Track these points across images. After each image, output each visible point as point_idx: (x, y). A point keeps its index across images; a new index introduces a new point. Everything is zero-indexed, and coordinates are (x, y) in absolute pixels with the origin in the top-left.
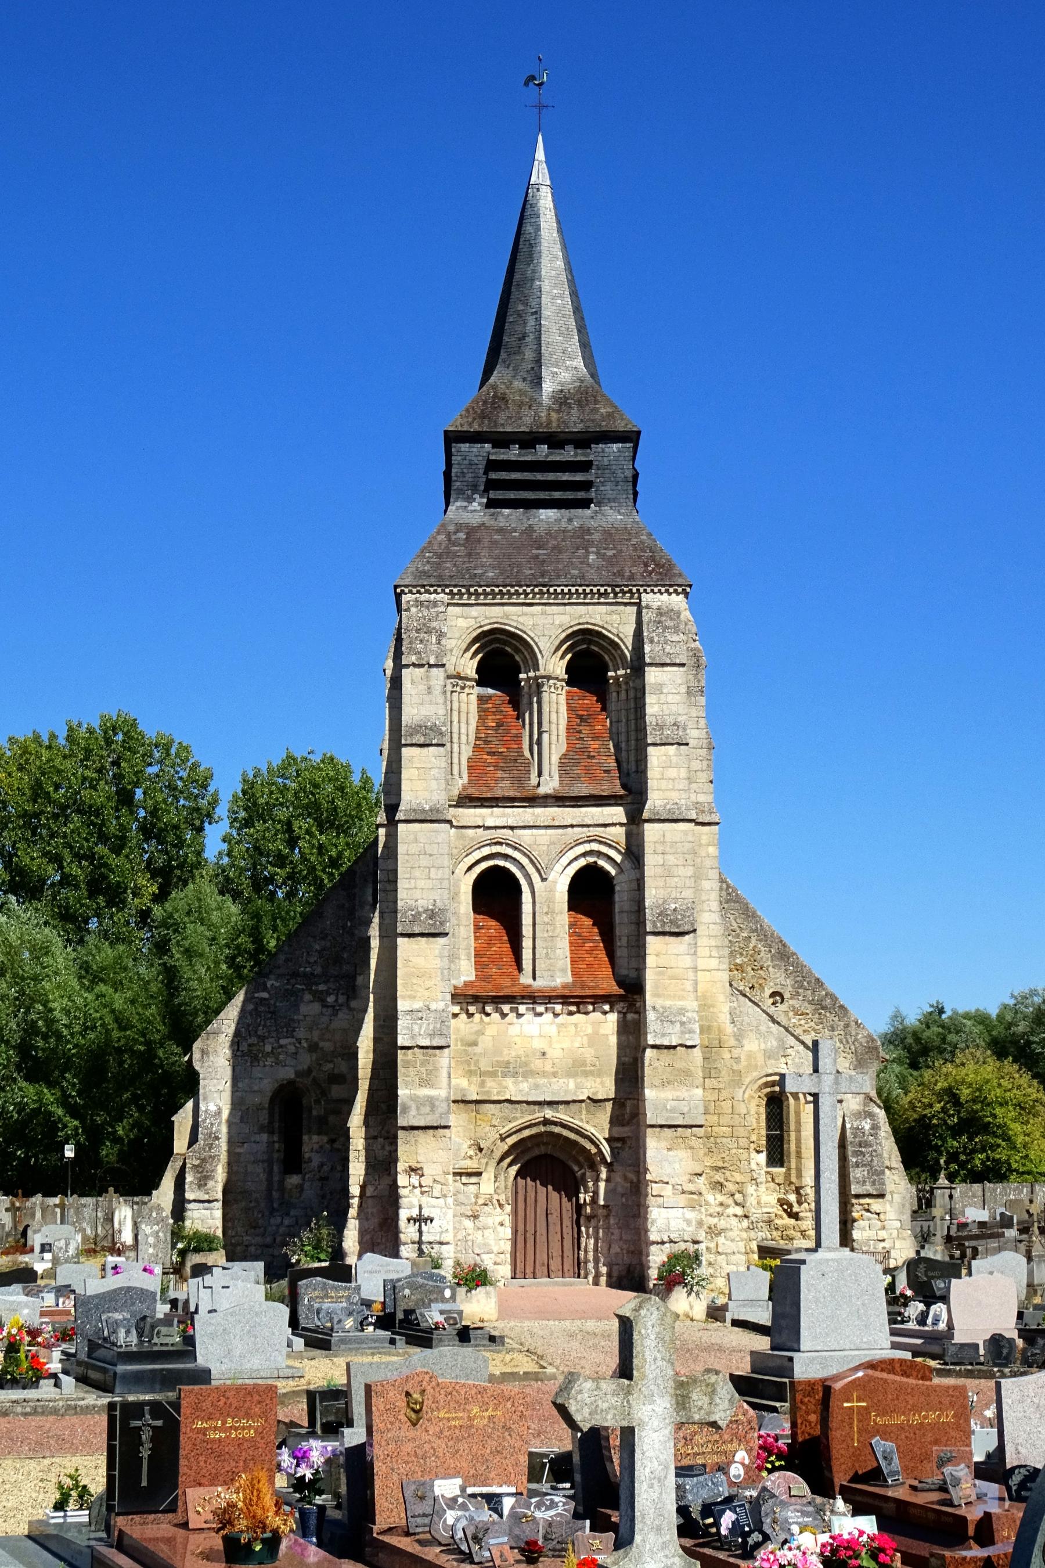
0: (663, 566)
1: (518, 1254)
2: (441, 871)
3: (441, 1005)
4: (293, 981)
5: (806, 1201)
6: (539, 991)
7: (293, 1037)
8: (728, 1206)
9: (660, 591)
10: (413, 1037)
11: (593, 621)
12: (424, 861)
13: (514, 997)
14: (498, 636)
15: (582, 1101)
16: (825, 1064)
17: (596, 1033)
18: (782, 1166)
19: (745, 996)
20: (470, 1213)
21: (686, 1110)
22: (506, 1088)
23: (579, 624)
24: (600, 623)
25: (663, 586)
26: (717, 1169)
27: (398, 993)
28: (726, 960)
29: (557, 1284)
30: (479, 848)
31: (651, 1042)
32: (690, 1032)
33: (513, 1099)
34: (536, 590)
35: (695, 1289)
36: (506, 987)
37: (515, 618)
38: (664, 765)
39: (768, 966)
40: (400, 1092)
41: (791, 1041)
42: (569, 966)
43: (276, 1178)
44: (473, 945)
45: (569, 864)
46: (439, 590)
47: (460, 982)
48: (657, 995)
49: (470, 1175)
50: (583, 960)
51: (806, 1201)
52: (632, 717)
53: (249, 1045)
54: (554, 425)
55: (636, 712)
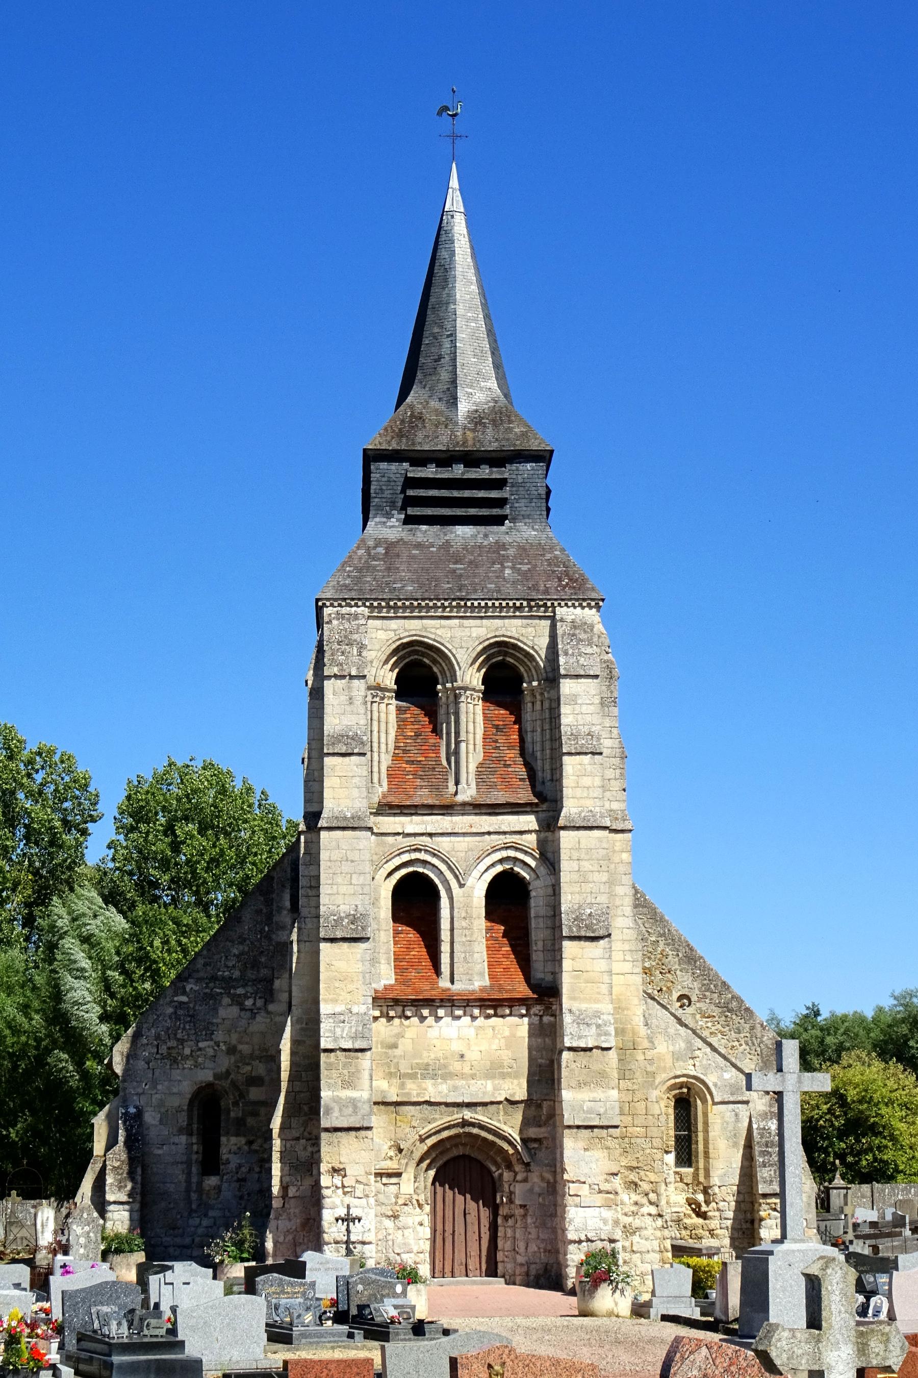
0: (577, 580)
1: (437, 1254)
2: (362, 878)
3: (362, 1009)
4: (211, 985)
5: (714, 1201)
6: (458, 994)
7: (212, 1040)
8: (642, 1205)
9: (573, 604)
10: (336, 1039)
11: (509, 634)
12: (346, 867)
13: (433, 1000)
14: (417, 648)
15: (499, 1103)
16: (789, 1064)
17: (513, 1035)
18: (690, 1166)
19: (653, 999)
20: (390, 1213)
21: (602, 1110)
22: (425, 1089)
23: (496, 636)
24: (516, 636)
25: (577, 600)
26: (632, 1169)
27: (321, 997)
28: (640, 964)
29: (475, 1283)
30: (399, 855)
31: (567, 1044)
32: (606, 1034)
33: (432, 1100)
34: (454, 603)
35: (620, 1286)
36: (426, 990)
37: (433, 630)
38: (578, 773)
39: (676, 970)
40: (323, 1094)
41: (699, 1043)
42: (487, 970)
43: (194, 1180)
44: (393, 949)
45: (486, 871)
46: (360, 603)
47: (380, 986)
48: (573, 999)
49: (390, 1175)
50: (500, 963)
51: (714, 1201)
52: (547, 727)
53: (169, 1048)
54: (470, 443)
55: (551, 722)
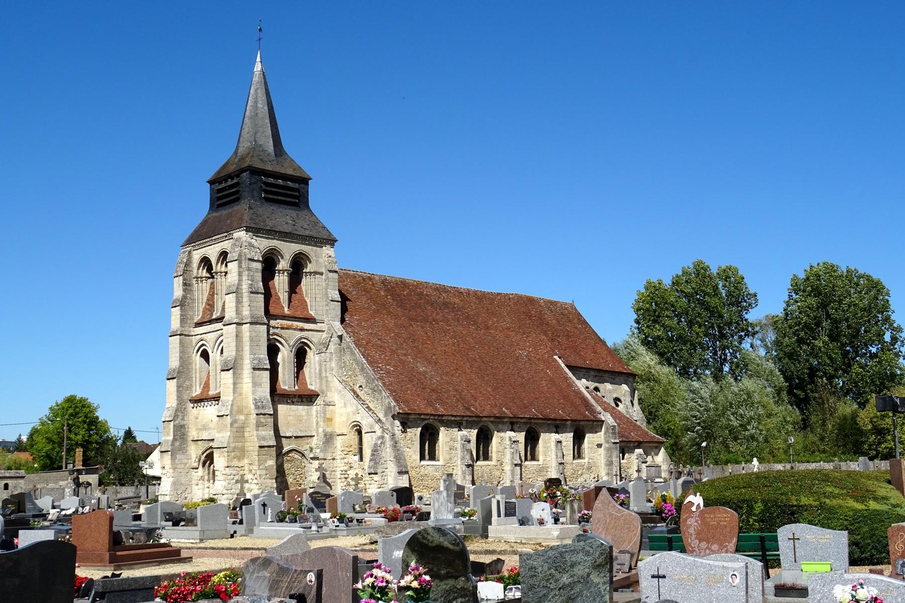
47: (194, 395)
